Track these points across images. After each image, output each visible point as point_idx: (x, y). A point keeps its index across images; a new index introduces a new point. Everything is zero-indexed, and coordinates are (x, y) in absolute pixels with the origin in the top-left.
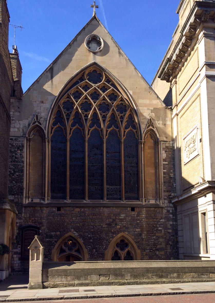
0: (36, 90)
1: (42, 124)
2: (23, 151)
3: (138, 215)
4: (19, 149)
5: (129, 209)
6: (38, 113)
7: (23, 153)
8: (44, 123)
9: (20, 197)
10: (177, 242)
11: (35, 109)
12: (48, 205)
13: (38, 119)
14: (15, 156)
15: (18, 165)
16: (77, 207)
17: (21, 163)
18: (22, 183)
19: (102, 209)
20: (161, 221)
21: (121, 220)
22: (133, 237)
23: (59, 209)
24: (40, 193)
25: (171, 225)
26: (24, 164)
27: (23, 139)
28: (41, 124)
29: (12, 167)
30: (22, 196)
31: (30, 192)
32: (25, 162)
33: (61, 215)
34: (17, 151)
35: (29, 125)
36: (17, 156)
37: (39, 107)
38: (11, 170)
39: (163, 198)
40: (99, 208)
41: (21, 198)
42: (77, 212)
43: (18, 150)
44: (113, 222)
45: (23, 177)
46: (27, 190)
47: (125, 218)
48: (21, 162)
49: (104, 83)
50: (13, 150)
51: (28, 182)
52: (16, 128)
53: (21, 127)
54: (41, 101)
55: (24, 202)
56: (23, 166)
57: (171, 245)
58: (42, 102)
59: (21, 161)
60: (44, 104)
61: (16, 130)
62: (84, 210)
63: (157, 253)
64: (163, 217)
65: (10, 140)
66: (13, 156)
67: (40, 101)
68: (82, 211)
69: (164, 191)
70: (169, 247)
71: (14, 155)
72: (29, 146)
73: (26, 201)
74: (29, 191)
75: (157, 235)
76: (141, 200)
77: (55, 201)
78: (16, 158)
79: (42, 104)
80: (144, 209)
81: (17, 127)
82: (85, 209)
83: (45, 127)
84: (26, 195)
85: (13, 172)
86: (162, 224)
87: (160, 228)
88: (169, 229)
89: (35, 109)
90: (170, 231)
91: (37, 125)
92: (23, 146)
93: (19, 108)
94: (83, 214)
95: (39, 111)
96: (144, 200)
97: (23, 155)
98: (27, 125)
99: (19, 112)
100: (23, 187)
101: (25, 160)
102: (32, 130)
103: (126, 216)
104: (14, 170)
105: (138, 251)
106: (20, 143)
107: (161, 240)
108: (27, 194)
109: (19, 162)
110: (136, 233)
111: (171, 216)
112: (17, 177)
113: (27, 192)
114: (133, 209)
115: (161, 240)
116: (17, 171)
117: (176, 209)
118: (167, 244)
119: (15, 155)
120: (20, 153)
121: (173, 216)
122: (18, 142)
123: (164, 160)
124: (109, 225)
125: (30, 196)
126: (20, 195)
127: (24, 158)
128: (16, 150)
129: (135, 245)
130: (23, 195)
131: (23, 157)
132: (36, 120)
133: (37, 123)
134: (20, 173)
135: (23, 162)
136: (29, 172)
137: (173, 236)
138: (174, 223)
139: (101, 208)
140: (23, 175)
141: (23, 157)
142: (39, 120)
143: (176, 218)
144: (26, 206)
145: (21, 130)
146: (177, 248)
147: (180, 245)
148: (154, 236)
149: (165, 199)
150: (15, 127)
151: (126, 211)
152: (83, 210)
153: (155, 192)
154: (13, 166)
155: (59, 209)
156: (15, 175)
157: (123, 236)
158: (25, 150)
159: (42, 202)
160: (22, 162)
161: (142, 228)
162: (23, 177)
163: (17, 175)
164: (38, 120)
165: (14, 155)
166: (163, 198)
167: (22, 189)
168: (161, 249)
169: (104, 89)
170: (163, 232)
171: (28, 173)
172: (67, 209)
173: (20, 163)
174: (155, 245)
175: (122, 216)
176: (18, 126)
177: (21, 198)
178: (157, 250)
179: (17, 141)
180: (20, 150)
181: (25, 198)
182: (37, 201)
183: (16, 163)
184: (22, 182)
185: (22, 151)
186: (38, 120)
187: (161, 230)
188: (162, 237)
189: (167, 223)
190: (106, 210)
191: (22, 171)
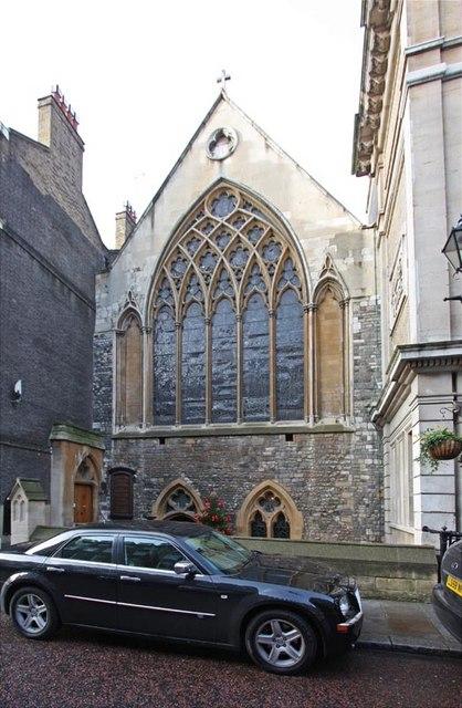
3: (299, 449)
10: (382, 499)
12: (146, 437)
16: (191, 437)
19: (231, 439)
20: (347, 457)
21: (267, 459)
22: (289, 489)
23: (162, 441)
25: (368, 466)
33: (165, 451)
39: (351, 413)
44: (251, 462)
47: (274, 454)
49: (238, 212)
55: (114, 433)
56: (111, 377)
57: (368, 506)
63: (337, 518)
64: (352, 448)
69: (355, 399)
70: (362, 508)
73: (116, 431)
75: (337, 485)
77: (158, 428)
80: (312, 436)
86: (348, 465)
87: (344, 473)
88: (364, 473)
90: (367, 477)
96: (311, 419)
101: (114, 366)
103: (277, 451)
105: (300, 514)
107: (345, 495)
110: (294, 480)
111: (369, 447)
114: (289, 437)
115: (345, 495)
117: (380, 433)
118: (359, 502)
121: (374, 448)
123: (357, 336)
124: (244, 466)
129: (292, 503)
135: (111, 369)
137: (373, 487)
138: (376, 462)
140: (111, 390)
143: (381, 451)
144: (115, 439)
146: (381, 511)
147: (386, 506)
148: (330, 486)
149: (356, 415)
155: (162, 442)
157: (268, 487)
158: (114, 350)
159: (139, 429)
161: (306, 470)
166: (351, 413)
167: (110, 412)
168: (347, 513)
169: (237, 219)
170: (350, 479)
171: (119, 385)
172: (176, 440)
174: (331, 503)
175: (269, 451)
178: (338, 513)
182: (130, 429)
187: (344, 476)
188: (348, 489)
189: (360, 461)
190: (240, 441)
191: (111, 385)
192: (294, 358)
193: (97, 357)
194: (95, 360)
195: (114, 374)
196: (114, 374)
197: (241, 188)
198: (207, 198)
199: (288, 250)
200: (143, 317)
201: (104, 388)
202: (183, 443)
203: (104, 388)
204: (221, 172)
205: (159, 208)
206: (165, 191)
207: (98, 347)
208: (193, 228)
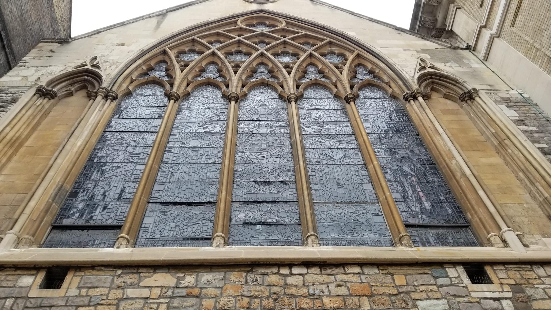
1: (102, 69)
5: (452, 272)
28: (98, 67)
40: (285, 271)
42: (157, 292)
58: (122, 45)
62: (197, 281)
67: (117, 44)
68: (184, 284)
76: (496, 240)
82: (207, 277)
94: (193, 301)
95: (106, 54)
139: (295, 270)
150: (18, 75)
151: (440, 281)
152: (190, 280)
202: (132, 286)
206: (185, 9)
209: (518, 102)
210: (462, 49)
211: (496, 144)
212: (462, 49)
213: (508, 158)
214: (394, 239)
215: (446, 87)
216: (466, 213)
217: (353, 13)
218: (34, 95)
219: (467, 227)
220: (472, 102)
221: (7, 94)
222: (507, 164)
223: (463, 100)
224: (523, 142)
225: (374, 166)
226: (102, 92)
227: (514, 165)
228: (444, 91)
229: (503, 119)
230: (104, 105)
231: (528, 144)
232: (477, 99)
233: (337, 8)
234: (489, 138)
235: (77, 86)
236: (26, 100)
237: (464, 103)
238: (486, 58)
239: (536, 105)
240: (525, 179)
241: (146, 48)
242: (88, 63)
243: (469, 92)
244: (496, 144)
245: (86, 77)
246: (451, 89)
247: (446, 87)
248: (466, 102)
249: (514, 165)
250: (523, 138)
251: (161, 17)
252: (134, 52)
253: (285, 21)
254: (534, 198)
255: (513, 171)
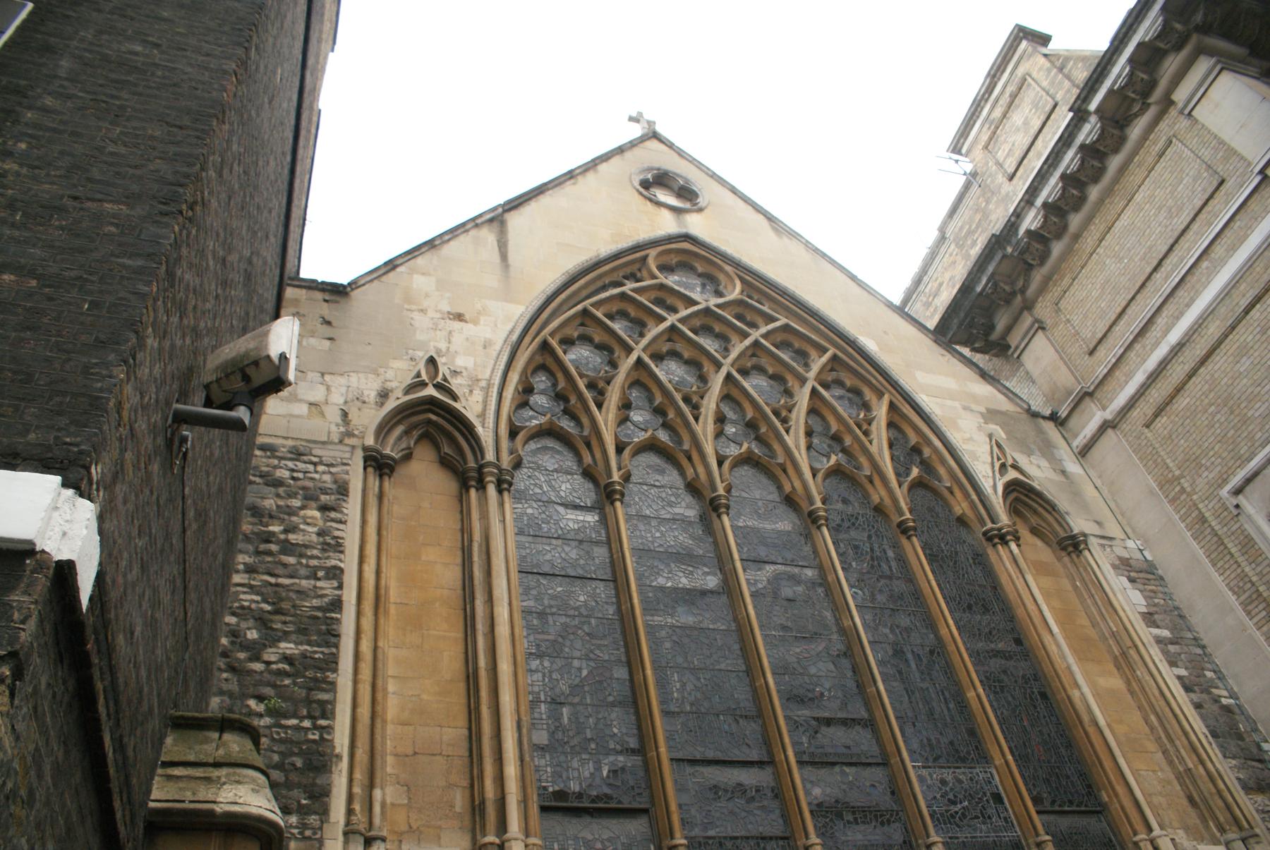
0: (423, 274)
1: (462, 398)
2: (342, 512)
4: (314, 504)
6: (438, 351)
7: (341, 526)
8: (478, 396)
9: (303, 826)
11: (420, 336)
13: (440, 375)
14: (282, 537)
15: (301, 593)
17: (319, 584)
18: (324, 716)
24: (452, 806)
26: (340, 587)
27: (347, 455)
28: (455, 397)
29: (247, 598)
30: (313, 819)
31: (377, 794)
32: (351, 580)
34: (302, 513)
35: (384, 395)
36: (292, 537)
37: (444, 333)
38: (244, 625)
41: (308, 833)
43: (303, 508)
45: (335, 670)
46: (358, 775)
48: (320, 574)
50: (269, 503)
51: (364, 711)
52: (301, 401)
53: (337, 398)
54: (453, 311)
56: (337, 604)
58: (459, 317)
59: (321, 568)
60: (470, 326)
61: (303, 409)
65: (258, 453)
66: (268, 538)
67: (449, 313)
71: (275, 528)
72: (381, 497)
74: (371, 785)
78: (287, 548)
79: (457, 325)
81: (312, 400)
83: (482, 416)
84: (350, 812)
85: (253, 635)
89: (420, 336)
91: (431, 401)
92: (342, 490)
93: (329, 323)
95: (443, 346)
97: (337, 533)
98: (371, 395)
99: (330, 339)
100: (325, 742)
102: (399, 422)
104: (262, 621)
106: (321, 468)
108: (357, 807)
109: (307, 578)
112: (280, 673)
113: (357, 790)
116: (291, 628)
119: (286, 531)
120: (321, 523)
122: (311, 468)
125: (377, 820)
126: (303, 811)
127: (342, 552)
128: (296, 503)
130: (324, 812)
131: (338, 547)
132: (424, 377)
133: (430, 391)
134: (309, 643)
135: (336, 574)
136: (376, 648)
140: (332, 663)
141: (340, 545)
142: (445, 379)
145: (333, 415)
153: (1185, 802)
154: (258, 598)
156: (273, 658)
158: (352, 507)
160: (327, 578)
162: (331, 676)
163: (287, 659)
164: (439, 379)
165: (273, 534)
171: (366, 646)
173: (319, 579)
176: (318, 394)
177: (308, 833)
179: (305, 458)
180: (324, 508)
181: (341, 838)
183: (286, 581)
184: (326, 710)
185: (333, 515)
186: (439, 379)
191: (331, 636)
192: (1006, 656)
193: (256, 512)
194: (246, 527)
195: (350, 596)
196: (350, 596)
197: (737, 264)
198: (653, 253)
199: (892, 407)
200: (485, 434)
201: (287, 647)
203: (287, 647)
204: (680, 223)
205: (515, 221)
207: (278, 483)
208: (629, 287)
209: (1141, 572)
210: (1044, 418)
211: (1117, 654)
212: (1044, 418)
213: (1134, 684)
214: (1026, 840)
215: (1035, 512)
216: (1099, 790)
217: (853, 278)
218: (365, 468)
219: (1098, 812)
220: (1078, 556)
221: (315, 464)
222: (1132, 693)
223: (1064, 549)
224: (1157, 661)
225: (978, 696)
226: (492, 474)
227: (1143, 700)
228: (1034, 520)
229: (1127, 608)
230: (501, 504)
231: (1164, 666)
232: (1086, 553)
233: (824, 256)
234: (1107, 639)
235: (416, 434)
236: (360, 485)
237: (1063, 554)
238: (1084, 452)
239: (1162, 578)
240: (1160, 729)
241: (515, 337)
242: (424, 377)
243: (1073, 537)
244: (1117, 654)
245: (433, 417)
246: (1045, 520)
247: (1035, 512)
248: (1069, 554)
249: (1143, 700)
250: (1156, 652)
251: (495, 224)
252: (498, 347)
253: (741, 279)
254: (1171, 763)
255: (1140, 708)
